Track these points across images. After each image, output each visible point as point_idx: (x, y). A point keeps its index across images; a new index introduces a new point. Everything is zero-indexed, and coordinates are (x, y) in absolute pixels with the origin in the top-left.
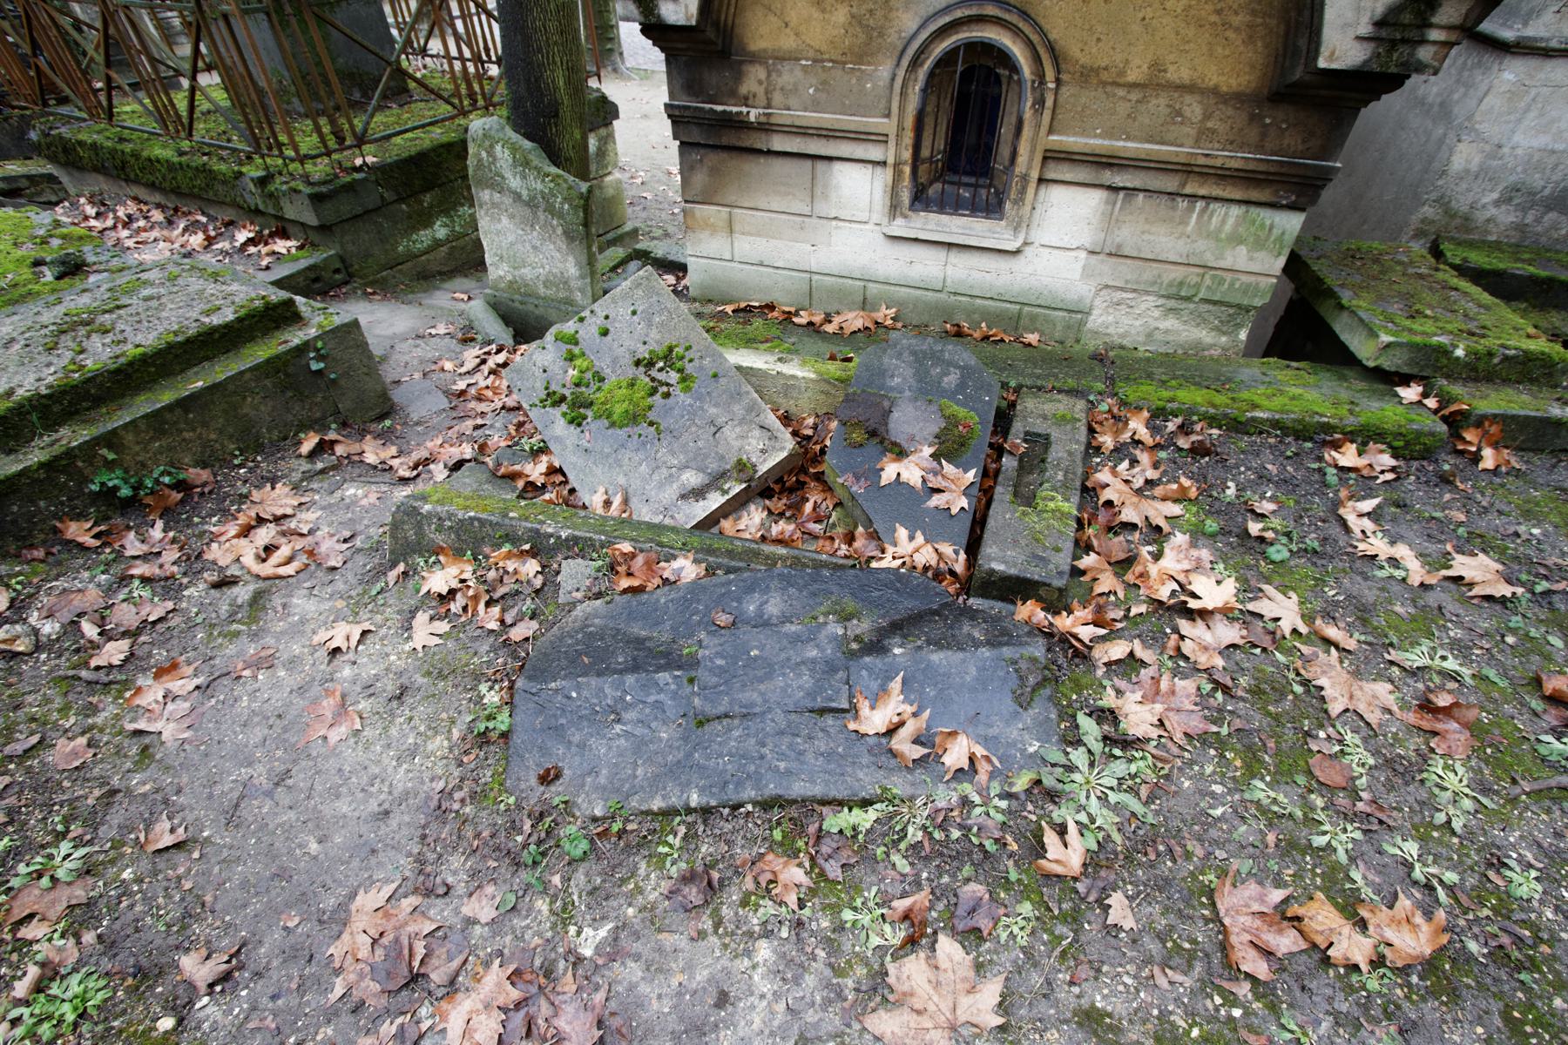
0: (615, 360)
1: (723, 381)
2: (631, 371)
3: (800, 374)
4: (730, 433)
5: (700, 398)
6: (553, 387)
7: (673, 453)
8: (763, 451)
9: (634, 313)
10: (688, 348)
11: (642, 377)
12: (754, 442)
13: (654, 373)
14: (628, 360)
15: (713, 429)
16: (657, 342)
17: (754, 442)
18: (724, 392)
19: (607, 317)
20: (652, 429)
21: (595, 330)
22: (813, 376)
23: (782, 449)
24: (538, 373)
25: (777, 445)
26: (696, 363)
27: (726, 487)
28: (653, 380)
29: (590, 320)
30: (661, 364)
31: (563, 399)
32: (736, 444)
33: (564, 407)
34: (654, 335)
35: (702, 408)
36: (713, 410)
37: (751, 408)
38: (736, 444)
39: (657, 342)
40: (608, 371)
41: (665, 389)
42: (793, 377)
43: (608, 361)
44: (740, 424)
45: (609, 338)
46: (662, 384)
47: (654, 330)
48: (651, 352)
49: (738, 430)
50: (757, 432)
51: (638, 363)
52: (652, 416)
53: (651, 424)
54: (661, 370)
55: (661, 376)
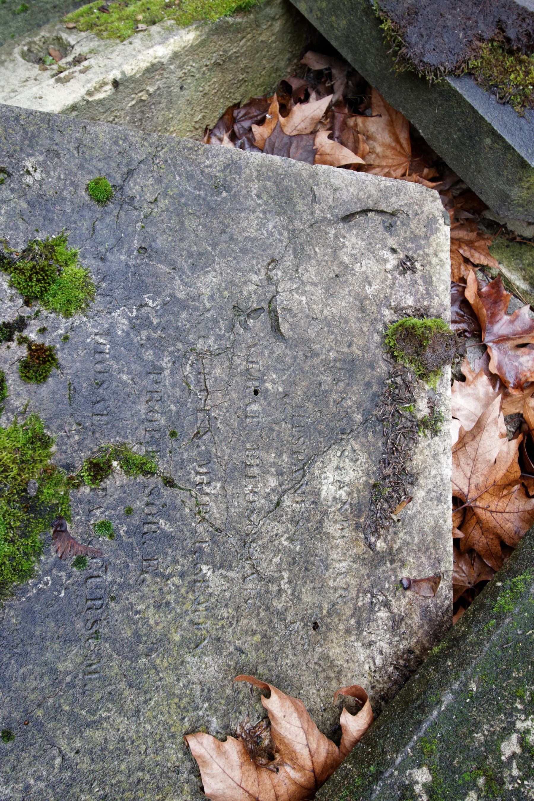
1: (142, 187)
3: (161, 52)
4: (301, 295)
5: (138, 286)
7: (240, 472)
8: (406, 266)
12: (368, 266)
15: (259, 325)
17: (368, 266)
18: (178, 212)
20: (118, 478)
22: (189, 37)
23: (430, 224)
25: (416, 227)
27: (423, 409)
32: (342, 304)
35: (173, 305)
36: (208, 283)
37: (282, 197)
38: (342, 304)
42: (154, 69)
44: (300, 254)
49: (311, 272)
50: (352, 241)
52: (69, 446)
53: (99, 470)
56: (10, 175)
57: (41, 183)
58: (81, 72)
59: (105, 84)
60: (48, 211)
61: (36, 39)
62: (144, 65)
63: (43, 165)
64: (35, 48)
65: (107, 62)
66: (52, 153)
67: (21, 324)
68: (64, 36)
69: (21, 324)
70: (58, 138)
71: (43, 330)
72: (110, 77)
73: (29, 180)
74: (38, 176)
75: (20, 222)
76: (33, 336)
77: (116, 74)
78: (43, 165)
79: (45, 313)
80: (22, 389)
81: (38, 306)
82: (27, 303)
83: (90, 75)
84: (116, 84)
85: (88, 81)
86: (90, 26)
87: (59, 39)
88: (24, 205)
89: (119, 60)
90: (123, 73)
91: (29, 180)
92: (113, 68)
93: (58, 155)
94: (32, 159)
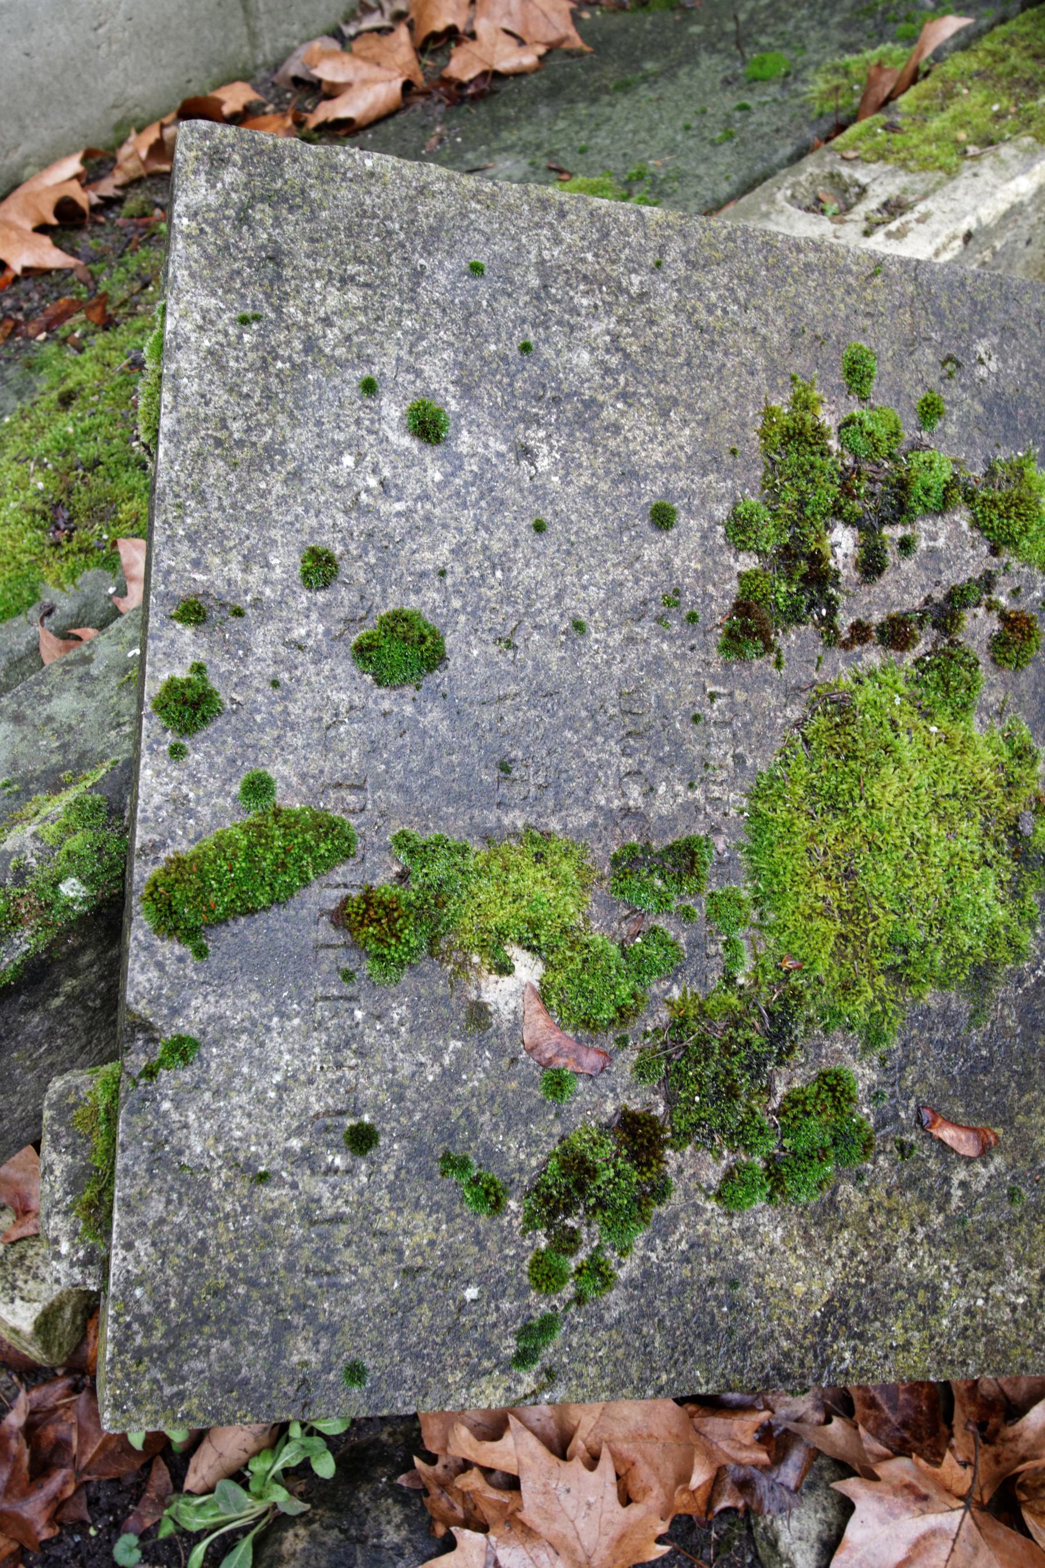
0: (638, 726)
2: (770, 693)
6: (524, 1154)
9: (427, 427)
10: (856, 375)
11: (839, 671)
13: (861, 604)
14: (690, 670)
16: (709, 460)
19: (320, 569)
21: (342, 685)
24: (338, 1186)
26: (962, 404)
28: (896, 634)
29: (243, 673)
30: (842, 543)
31: (639, 1136)
33: (694, 1167)
34: (656, 444)
39: (709, 460)
40: (669, 797)
41: (978, 626)
42: (1015, 211)
43: (608, 752)
45: (467, 651)
46: (946, 613)
47: (637, 424)
48: (740, 529)
51: (749, 627)
54: (871, 565)
55: (905, 588)
56: (959, 365)
57: (997, 376)
58: (919, 221)
59: (954, 237)
60: (1009, 415)
61: (802, 178)
62: (1003, 207)
63: (998, 349)
64: (800, 192)
65: (952, 204)
66: (1007, 333)
67: (988, 582)
68: (845, 171)
69: (988, 582)
70: (1014, 311)
71: (1015, 592)
72: (963, 227)
73: (982, 371)
74: (993, 365)
75: (976, 433)
76: (1003, 600)
77: (968, 223)
78: (998, 349)
79: (1015, 564)
80: (994, 677)
81: (1007, 555)
82: (994, 551)
83: (934, 225)
84: (968, 236)
85: (936, 234)
86: (881, 156)
87: (834, 177)
88: (980, 409)
89: (969, 201)
90: (979, 220)
91: (982, 371)
92: (965, 214)
93: (1014, 336)
94: (985, 342)
